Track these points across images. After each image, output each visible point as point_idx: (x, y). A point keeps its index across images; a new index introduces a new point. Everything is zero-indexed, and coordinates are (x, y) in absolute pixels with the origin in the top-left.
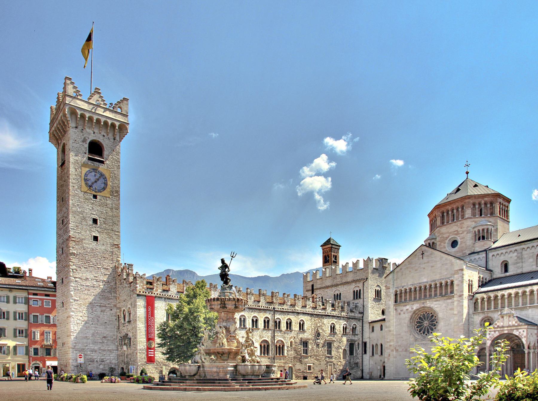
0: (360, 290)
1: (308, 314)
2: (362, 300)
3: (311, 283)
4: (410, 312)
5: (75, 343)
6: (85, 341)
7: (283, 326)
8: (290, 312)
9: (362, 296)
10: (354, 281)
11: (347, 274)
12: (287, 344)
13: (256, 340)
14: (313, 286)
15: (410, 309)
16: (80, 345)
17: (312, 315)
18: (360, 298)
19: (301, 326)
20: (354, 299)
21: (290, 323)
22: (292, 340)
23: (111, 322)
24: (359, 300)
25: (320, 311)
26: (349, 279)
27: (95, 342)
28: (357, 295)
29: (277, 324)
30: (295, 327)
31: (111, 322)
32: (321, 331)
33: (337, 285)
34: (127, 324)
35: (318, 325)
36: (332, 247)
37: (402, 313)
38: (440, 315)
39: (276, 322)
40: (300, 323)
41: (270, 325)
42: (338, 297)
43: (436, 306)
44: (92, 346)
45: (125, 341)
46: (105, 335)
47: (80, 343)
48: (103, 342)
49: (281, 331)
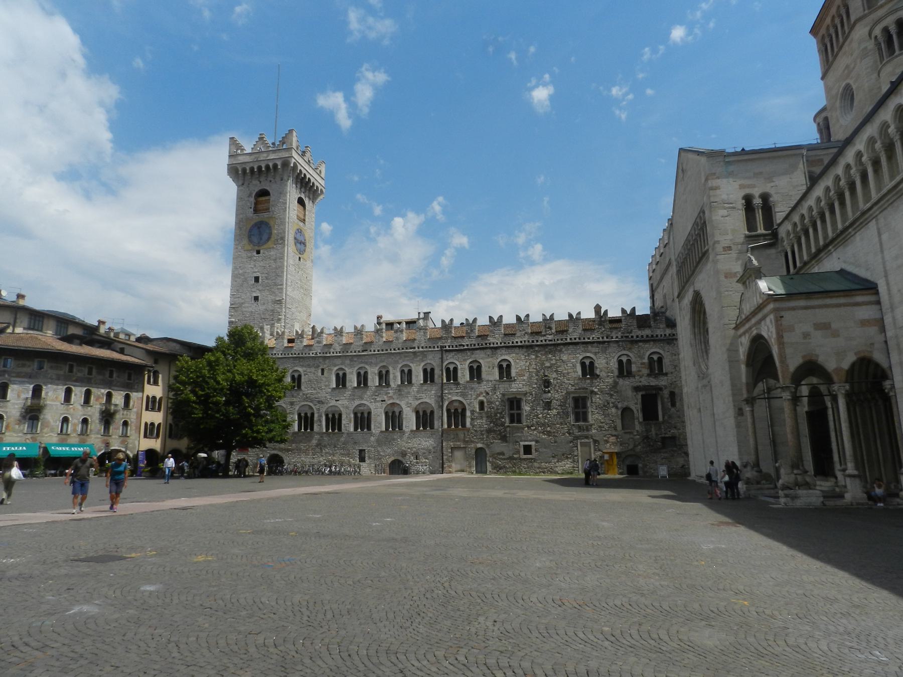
1: (519, 347)
7: (464, 375)
8: (477, 349)
12: (472, 405)
13: (408, 403)
17: (529, 347)
19: (505, 370)
22: (481, 398)
25: (550, 337)
29: (452, 374)
30: (491, 374)
35: (548, 364)
39: (448, 370)
41: (436, 377)
49: (458, 384)
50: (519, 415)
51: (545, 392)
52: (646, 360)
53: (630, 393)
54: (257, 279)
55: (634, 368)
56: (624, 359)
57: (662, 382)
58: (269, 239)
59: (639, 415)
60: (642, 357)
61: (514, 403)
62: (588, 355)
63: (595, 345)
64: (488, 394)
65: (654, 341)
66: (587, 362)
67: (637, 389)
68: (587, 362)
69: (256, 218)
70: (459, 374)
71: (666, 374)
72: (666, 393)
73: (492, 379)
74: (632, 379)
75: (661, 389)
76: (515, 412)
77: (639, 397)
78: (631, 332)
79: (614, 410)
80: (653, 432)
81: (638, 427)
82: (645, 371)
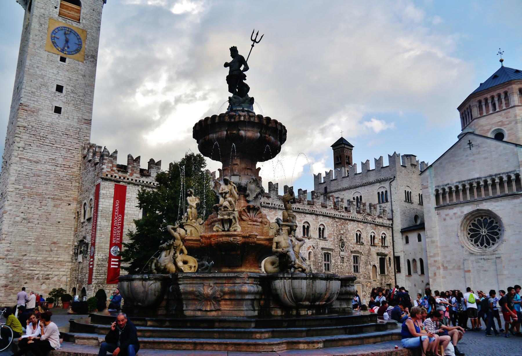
0: (386, 191)
2: (389, 203)
3: (324, 186)
4: (460, 217)
5: (8, 251)
6: (23, 248)
9: (389, 199)
10: (379, 181)
11: (370, 172)
14: (326, 188)
15: (459, 213)
16: (15, 254)
17: (334, 218)
18: (387, 201)
19: (321, 232)
20: (379, 203)
21: (308, 227)
22: (310, 250)
23: (67, 222)
24: (386, 204)
25: (343, 214)
26: (372, 179)
27: (39, 250)
28: (383, 198)
30: (314, 233)
31: (67, 222)
32: (345, 240)
33: (356, 187)
34: (86, 224)
35: (342, 232)
36: (344, 147)
37: (447, 218)
38: (505, 220)
40: (320, 229)
42: (359, 200)
43: (497, 208)
44: (32, 256)
45: (81, 248)
46: (55, 240)
47: (14, 251)
48: (51, 250)
50: (328, 265)
51: (342, 251)
52: (381, 238)
53: (375, 256)
54: (59, 89)
55: (376, 241)
56: (373, 235)
57: (385, 251)
58: (77, 51)
59: (378, 270)
60: (379, 235)
61: (327, 256)
62: (359, 229)
63: (362, 223)
64: (314, 248)
65: (383, 226)
66: (358, 233)
67: (378, 254)
68: (358, 233)
69: (62, 22)
70: (298, 230)
71: (387, 247)
72: (387, 258)
73: (316, 237)
74: (376, 248)
75: (386, 255)
76: (327, 263)
77: (379, 259)
78: (375, 219)
79: (370, 266)
80: (384, 281)
81: (379, 277)
82: (381, 244)
